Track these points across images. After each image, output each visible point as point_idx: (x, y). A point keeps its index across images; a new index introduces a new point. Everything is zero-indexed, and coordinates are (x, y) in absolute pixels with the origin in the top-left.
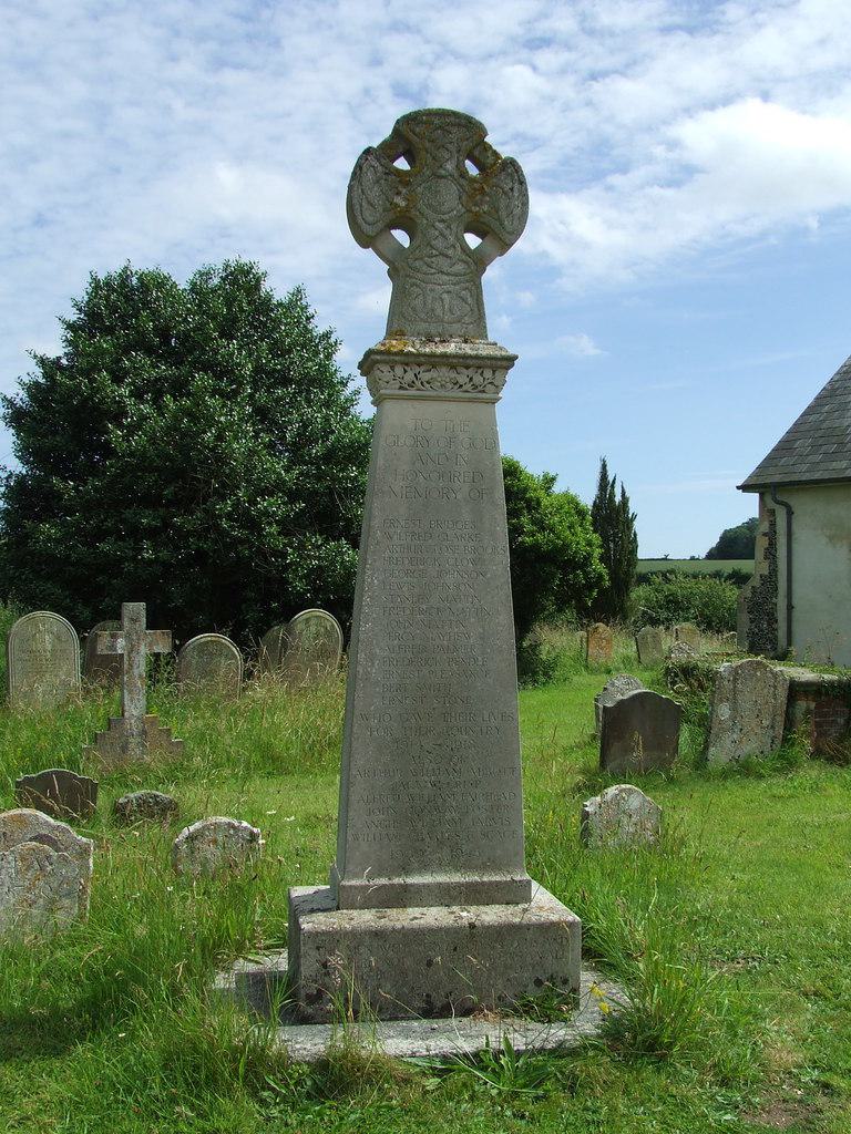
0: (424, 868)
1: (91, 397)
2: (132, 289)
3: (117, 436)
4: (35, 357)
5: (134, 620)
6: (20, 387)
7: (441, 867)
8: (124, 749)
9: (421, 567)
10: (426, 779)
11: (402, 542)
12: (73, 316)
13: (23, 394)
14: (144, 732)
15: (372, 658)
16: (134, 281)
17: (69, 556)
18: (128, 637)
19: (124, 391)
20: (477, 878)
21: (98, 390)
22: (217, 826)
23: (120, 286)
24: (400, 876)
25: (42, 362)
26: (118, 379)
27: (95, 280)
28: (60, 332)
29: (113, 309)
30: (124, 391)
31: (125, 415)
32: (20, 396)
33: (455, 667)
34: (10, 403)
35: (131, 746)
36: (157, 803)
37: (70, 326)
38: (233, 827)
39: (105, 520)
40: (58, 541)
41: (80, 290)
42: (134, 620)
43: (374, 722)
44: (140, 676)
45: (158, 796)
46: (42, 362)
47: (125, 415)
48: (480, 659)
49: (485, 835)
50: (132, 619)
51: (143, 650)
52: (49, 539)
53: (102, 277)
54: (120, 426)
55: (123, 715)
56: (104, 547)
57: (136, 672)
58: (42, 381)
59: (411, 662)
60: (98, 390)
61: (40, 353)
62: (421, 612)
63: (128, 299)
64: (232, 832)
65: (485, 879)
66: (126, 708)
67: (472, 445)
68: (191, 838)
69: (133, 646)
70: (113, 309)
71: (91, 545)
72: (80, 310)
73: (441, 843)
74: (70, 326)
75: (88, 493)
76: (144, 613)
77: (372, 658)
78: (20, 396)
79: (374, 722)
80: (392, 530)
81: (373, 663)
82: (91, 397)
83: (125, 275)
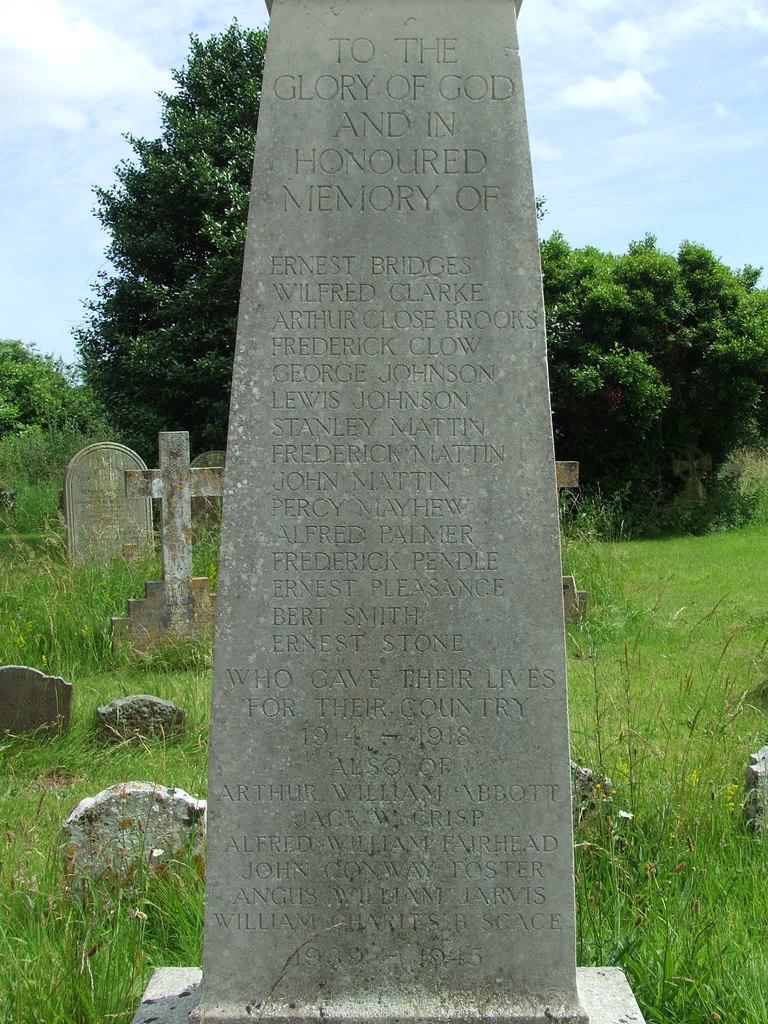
0: (365, 984)
1: (190, 184)
2: (241, 54)
3: (216, 230)
4: (132, 141)
5: (174, 455)
6: (118, 178)
7: (399, 983)
8: (166, 621)
9: (354, 358)
10: (369, 805)
11: (312, 305)
12: (174, 90)
13: (122, 187)
14: (191, 600)
15: (249, 553)
16: (244, 43)
17: (164, 376)
18: (167, 476)
19: (227, 175)
20: (473, 1010)
21: (197, 176)
22: (131, 800)
23: (225, 50)
24: (313, 1000)
25: (140, 147)
26: (220, 163)
27: (197, 45)
28: (159, 109)
29: (217, 78)
30: (227, 175)
31: (228, 204)
32: (118, 189)
33: (427, 573)
34: (107, 198)
35: (174, 619)
36: (153, 713)
37: (171, 103)
38: (160, 800)
39: (207, 332)
40: (151, 357)
41: (181, 57)
42: (174, 455)
43: (256, 688)
44: (184, 528)
45: (155, 704)
46: (140, 147)
47: (228, 204)
48: (481, 554)
49: (493, 922)
50: (172, 453)
51: (188, 493)
52: (141, 355)
53: (204, 40)
54: (219, 217)
55: (163, 578)
56: (203, 363)
57: (178, 522)
58: (139, 168)
59: (333, 562)
60: (197, 176)
61: (137, 137)
62: (354, 454)
63: (235, 66)
64: (156, 808)
65: (491, 1013)
66: (167, 569)
67: (464, 90)
68: (89, 818)
69: (173, 488)
70: (217, 78)
71: (189, 362)
72: (182, 83)
73: (399, 936)
74: (171, 103)
75: (186, 298)
76: (186, 445)
77: (249, 553)
78: (118, 189)
79: (256, 688)
80: (291, 279)
81: (252, 565)
82: (190, 184)
83: (231, 40)
